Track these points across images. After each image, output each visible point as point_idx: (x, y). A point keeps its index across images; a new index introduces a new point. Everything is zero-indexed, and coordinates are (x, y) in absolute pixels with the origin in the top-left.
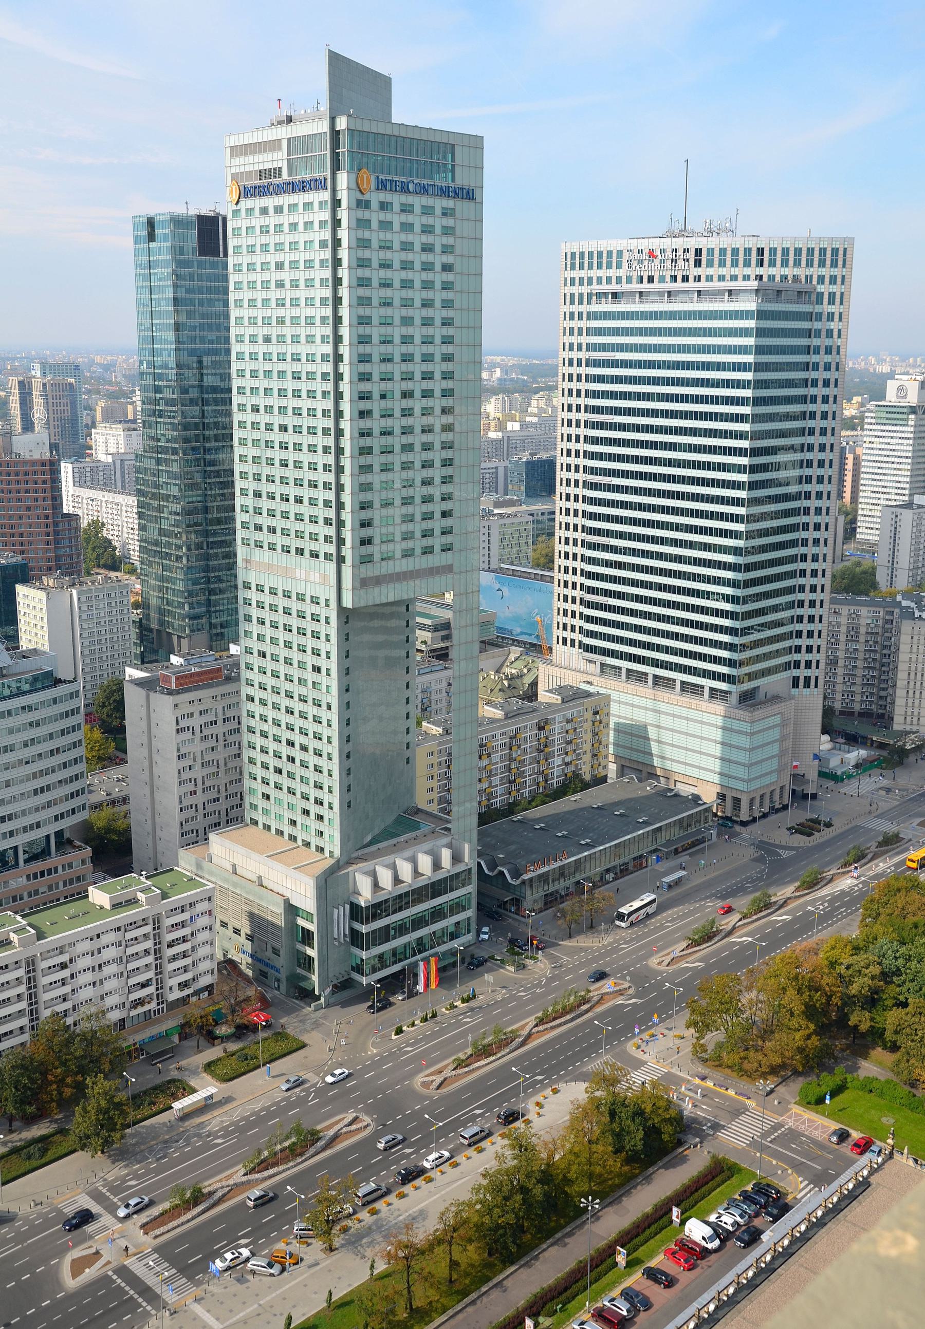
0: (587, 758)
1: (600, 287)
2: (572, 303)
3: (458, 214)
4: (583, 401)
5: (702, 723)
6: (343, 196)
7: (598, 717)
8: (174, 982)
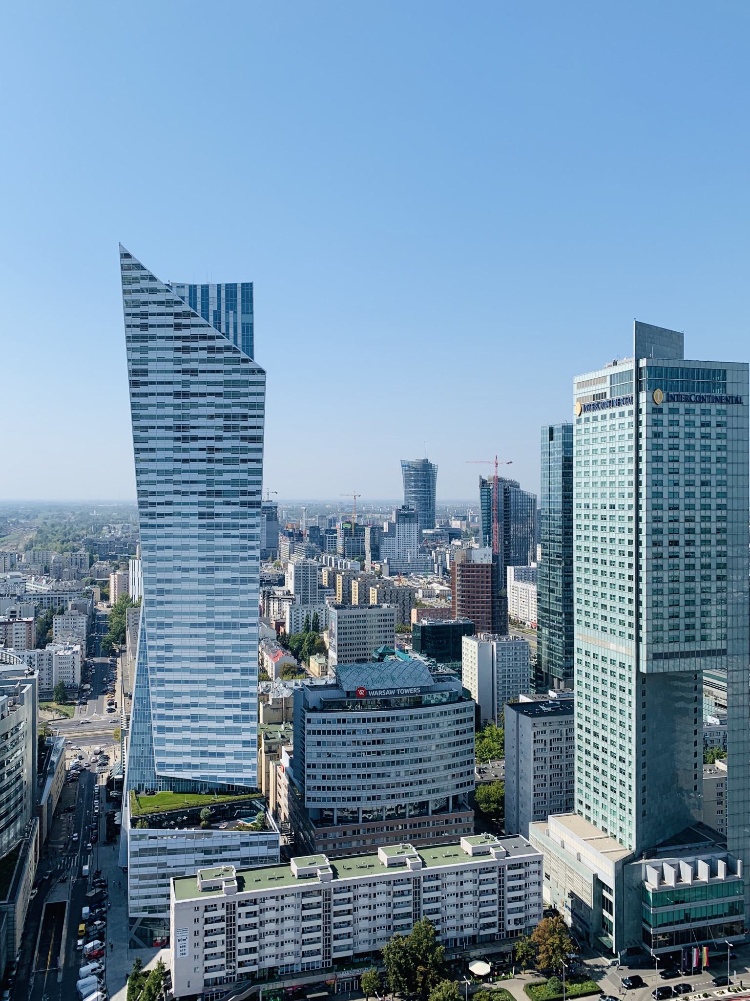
3: (729, 413)
6: (643, 406)
8: (511, 917)
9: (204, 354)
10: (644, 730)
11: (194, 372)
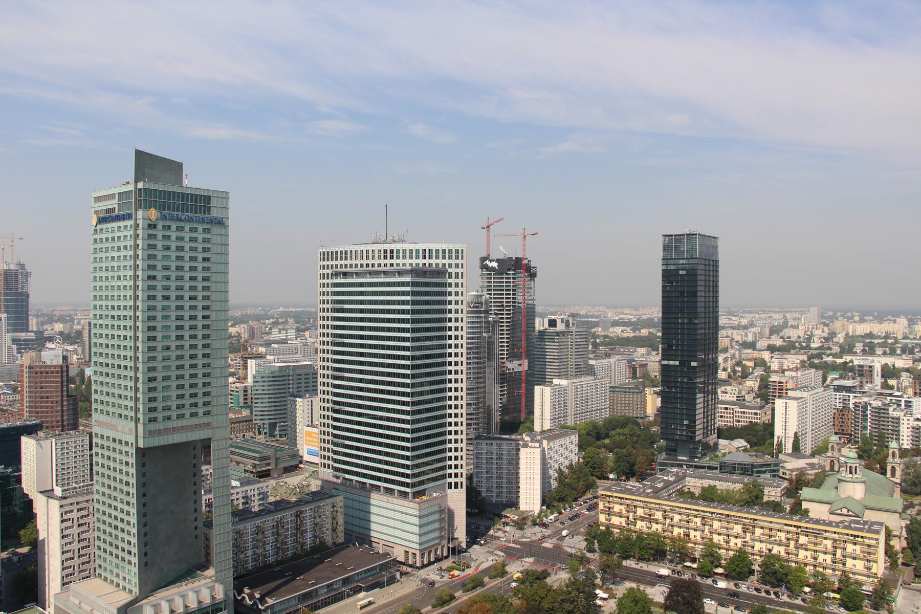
0: (329, 532)
1: (336, 270)
2: (324, 278)
4: (330, 331)
5: (394, 510)
7: (335, 509)
10: (144, 495)
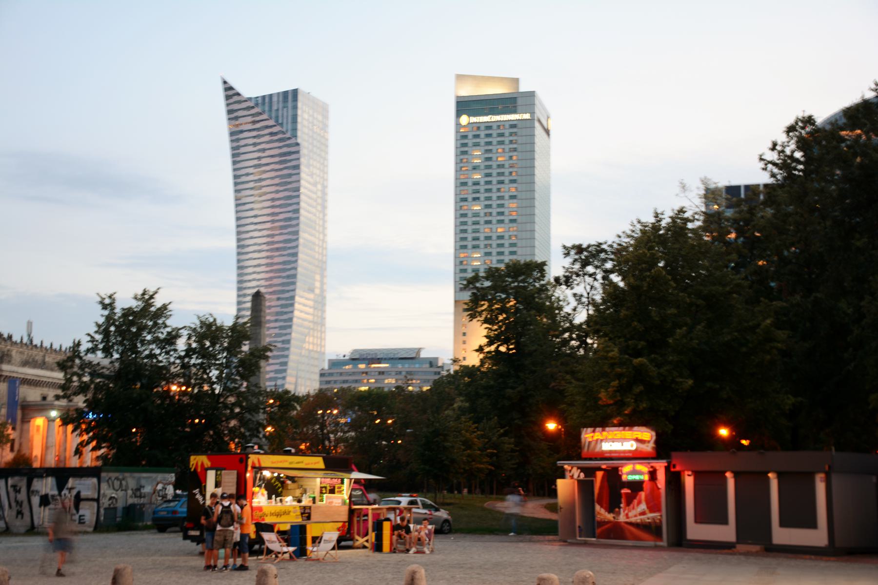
9: (267, 138)
11: (264, 150)
